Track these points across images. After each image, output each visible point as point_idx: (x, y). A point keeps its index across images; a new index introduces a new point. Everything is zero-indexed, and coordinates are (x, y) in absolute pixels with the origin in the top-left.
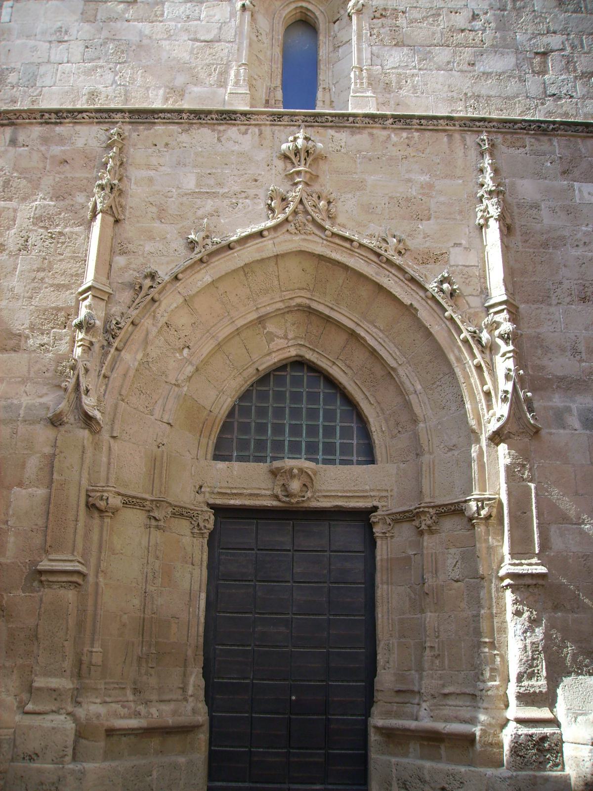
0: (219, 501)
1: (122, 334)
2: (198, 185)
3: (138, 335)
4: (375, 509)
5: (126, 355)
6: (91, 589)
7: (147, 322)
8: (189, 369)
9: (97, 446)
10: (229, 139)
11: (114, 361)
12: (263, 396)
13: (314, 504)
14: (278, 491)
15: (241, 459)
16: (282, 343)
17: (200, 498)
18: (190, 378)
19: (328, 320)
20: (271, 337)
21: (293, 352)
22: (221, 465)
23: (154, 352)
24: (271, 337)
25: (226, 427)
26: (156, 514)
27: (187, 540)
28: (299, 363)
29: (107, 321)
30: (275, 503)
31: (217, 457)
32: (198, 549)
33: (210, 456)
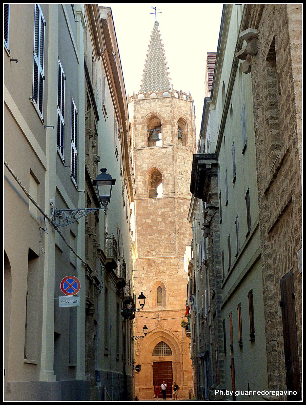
0: (153, 361)
1: (140, 344)
2: (147, 322)
3: (142, 343)
4: (172, 361)
5: (140, 346)
6: (139, 374)
7: (142, 342)
8: (148, 346)
9: (138, 357)
10: (150, 315)
11: (139, 347)
12: (158, 346)
13: (165, 361)
14: (160, 360)
15: (156, 355)
16: (160, 340)
17: (151, 361)
18: (148, 347)
19: (165, 338)
20: (158, 339)
21: (161, 341)
22: (153, 357)
23: (144, 345)
24: (158, 339)
25: (154, 351)
26: (146, 364)
27: (150, 366)
28: (162, 342)
29: (138, 342)
30: (160, 361)
31: (153, 355)
32: (151, 368)
33: (152, 355)
